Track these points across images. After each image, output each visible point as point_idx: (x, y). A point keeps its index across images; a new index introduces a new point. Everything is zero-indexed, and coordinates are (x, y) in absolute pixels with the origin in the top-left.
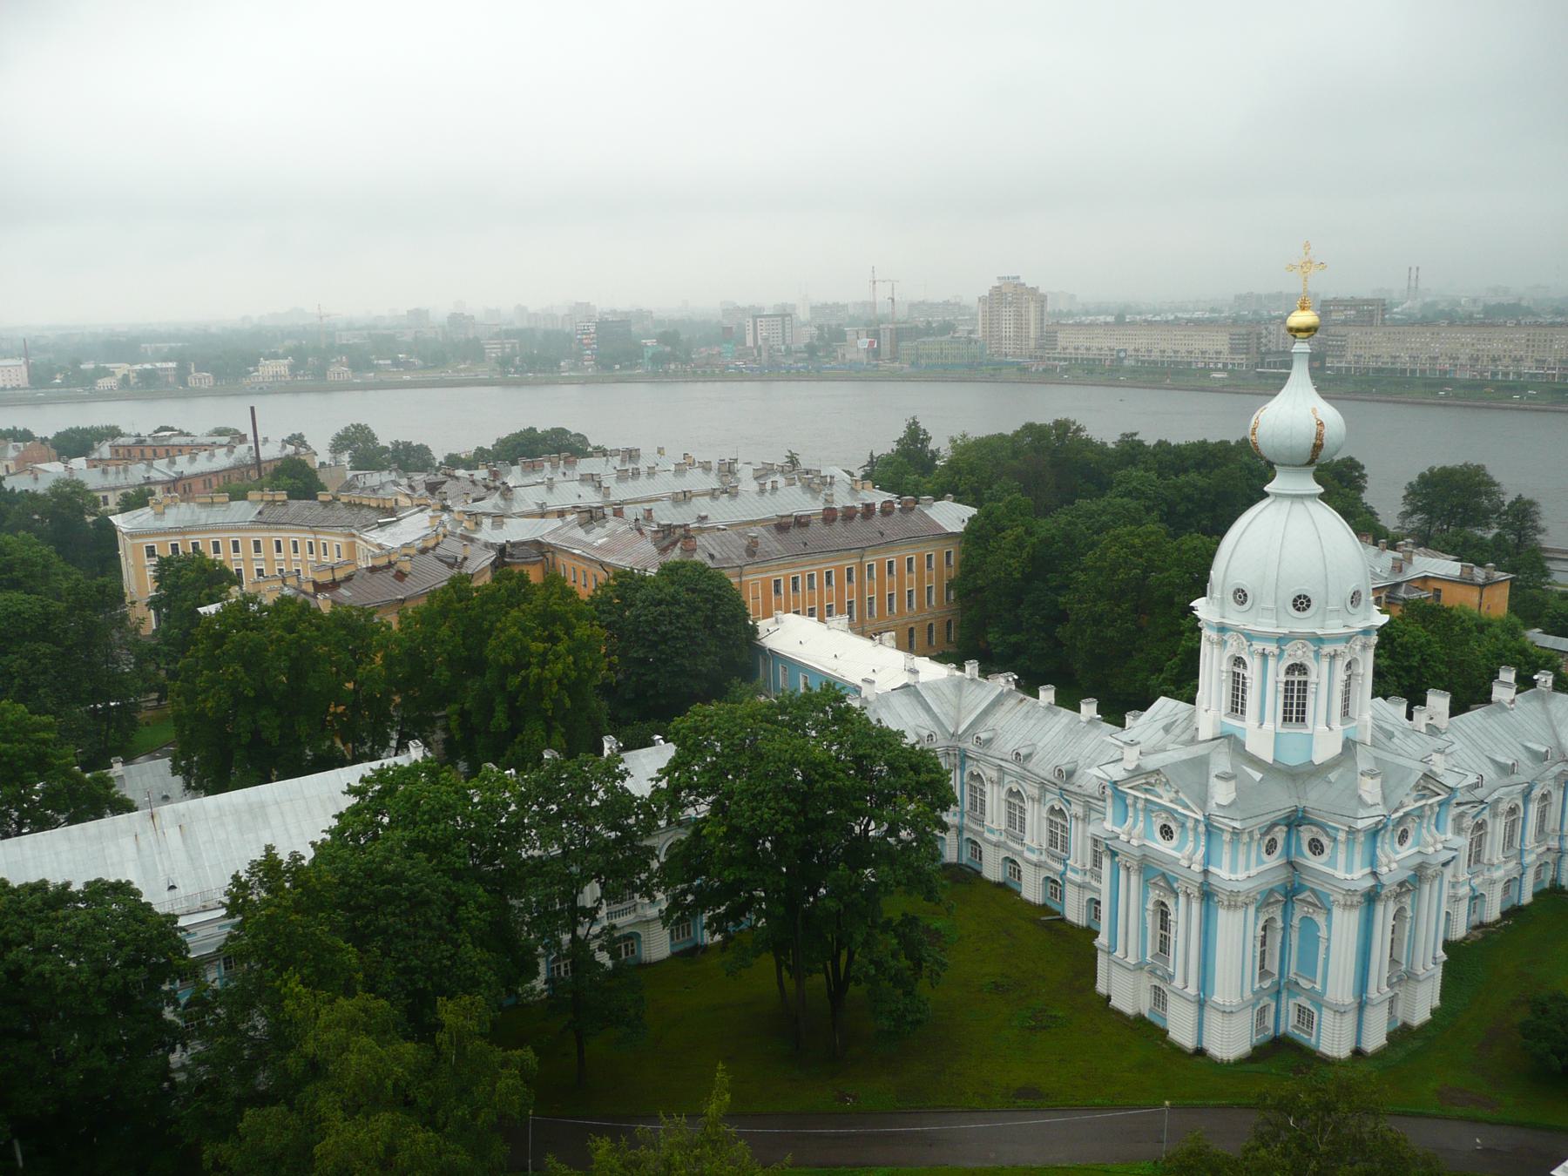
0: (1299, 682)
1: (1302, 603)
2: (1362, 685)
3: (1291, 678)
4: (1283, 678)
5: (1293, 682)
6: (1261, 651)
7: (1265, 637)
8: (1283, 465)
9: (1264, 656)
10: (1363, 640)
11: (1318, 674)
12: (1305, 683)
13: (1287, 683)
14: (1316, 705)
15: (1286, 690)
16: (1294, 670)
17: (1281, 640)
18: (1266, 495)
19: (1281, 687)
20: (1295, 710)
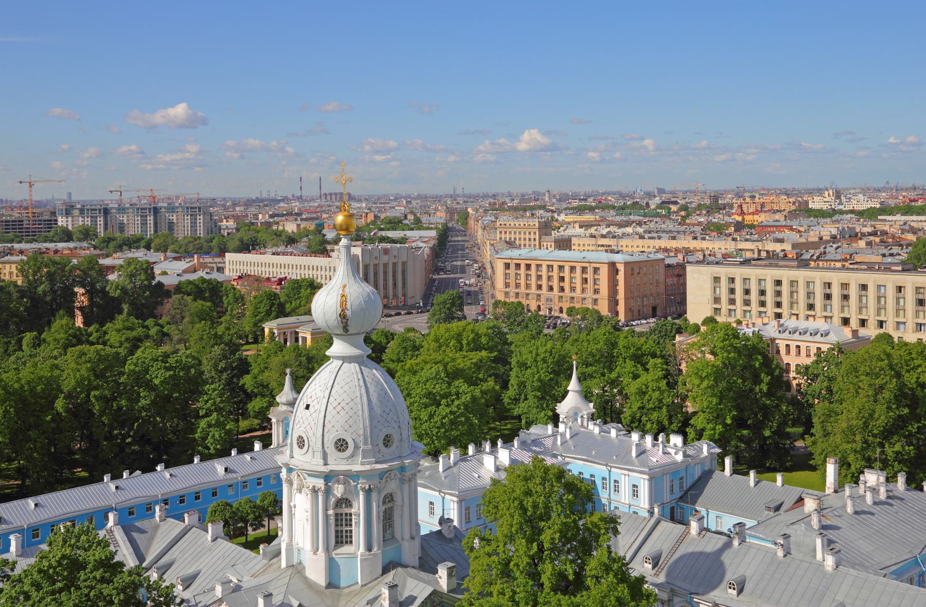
0: (346, 514)
1: (341, 445)
2: (402, 516)
3: (339, 511)
4: (331, 512)
5: (342, 514)
6: (311, 487)
7: (314, 474)
8: (337, 335)
9: (315, 491)
10: (400, 476)
11: (359, 507)
12: (351, 515)
13: (337, 515)
14: (359, 532)
15: (336, 520)
16: (342, 503)
17: (328, 477)
18: (328, 358)
19: (332, 520)
20: (342, 538)
